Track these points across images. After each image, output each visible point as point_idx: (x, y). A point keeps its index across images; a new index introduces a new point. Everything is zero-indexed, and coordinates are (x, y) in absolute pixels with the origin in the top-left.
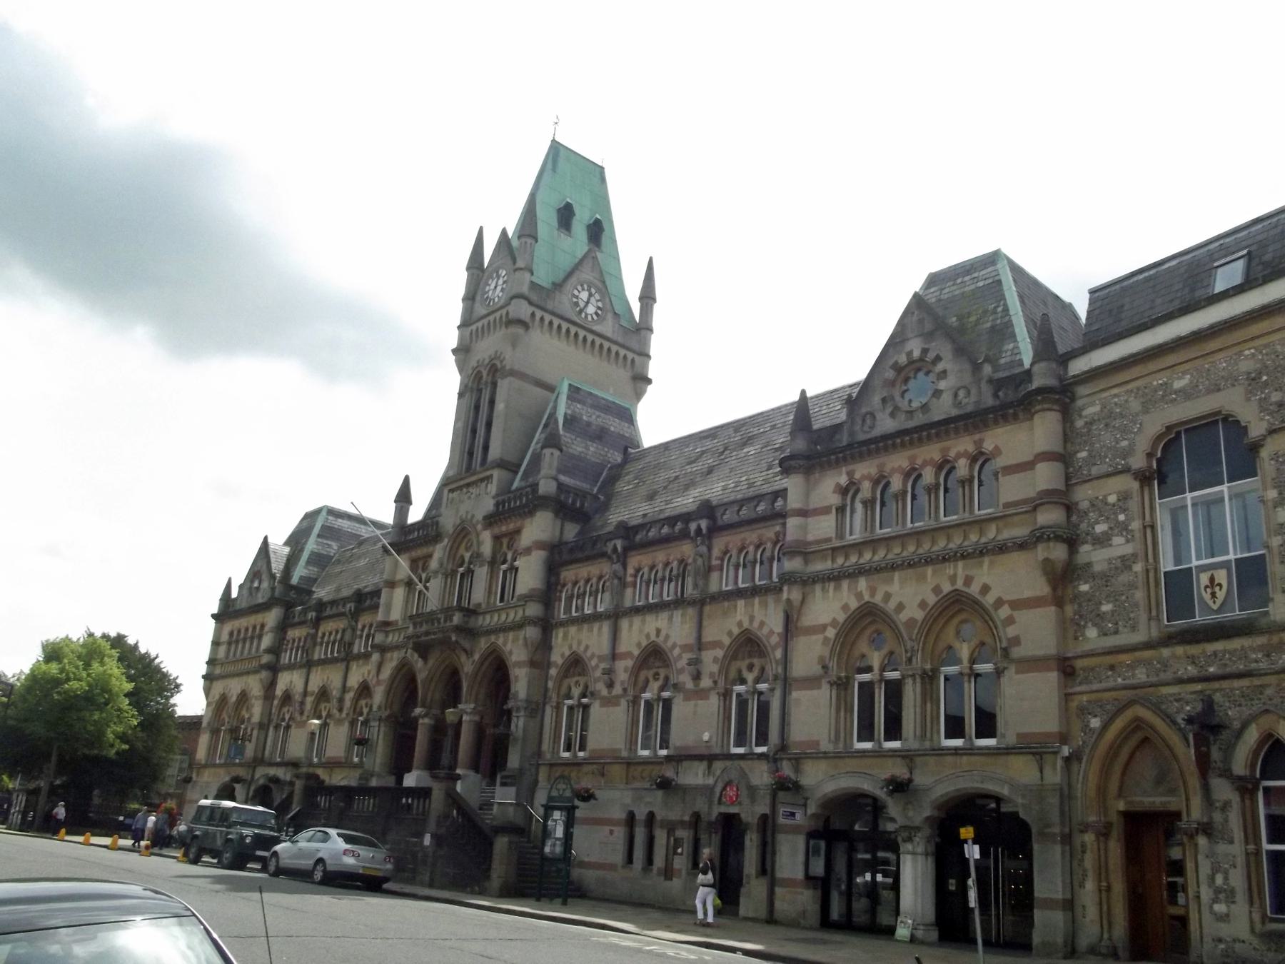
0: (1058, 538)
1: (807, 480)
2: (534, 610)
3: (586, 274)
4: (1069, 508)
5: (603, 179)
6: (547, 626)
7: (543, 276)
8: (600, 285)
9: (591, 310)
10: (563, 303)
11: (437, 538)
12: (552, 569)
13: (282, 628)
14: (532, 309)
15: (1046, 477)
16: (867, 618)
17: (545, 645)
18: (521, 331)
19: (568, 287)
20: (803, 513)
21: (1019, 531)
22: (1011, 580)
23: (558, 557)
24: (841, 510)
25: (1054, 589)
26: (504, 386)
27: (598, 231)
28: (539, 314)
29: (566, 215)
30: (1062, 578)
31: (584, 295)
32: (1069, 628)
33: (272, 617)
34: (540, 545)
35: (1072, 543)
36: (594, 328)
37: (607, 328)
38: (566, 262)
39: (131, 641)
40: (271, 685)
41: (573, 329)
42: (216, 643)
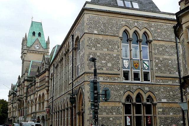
0: (46, 87)
1: (38, 78)
2: (25, 95)
3: (37, 42)
4: (49, 83)
5: (41, 25)
6: (27, 97)
7: (29, 44)
8: (39, 44)
9: (38, 48)
10: (33, 48)
11: (20, 85)
12: (27, 89)
13: (13, 97)
14: (27, 51)
15: (47, 79)
16: (40, 95)
17: (26, 99)
18: (25, 54)
19: (33, 46)
20: (38, 83)
21: (44, 87)
22: (45, 92)
23: (28, 87)
24: (40, 82)
25: (47, 92)
26: (25, 62)
27: (40, 34)
28: (28, 51)
29: (34, 33)
30: (48, 91)
31: (36, 46)
32: (48, 97)
33: (12, 95)
34: (26, 86)
35: (49, 87)
36: (39, 50)
37: (41, 50)
38: (33, 41)
39: (5, 100)
40: (13, 106)
41: (35, 52)
42: (9, 100)
